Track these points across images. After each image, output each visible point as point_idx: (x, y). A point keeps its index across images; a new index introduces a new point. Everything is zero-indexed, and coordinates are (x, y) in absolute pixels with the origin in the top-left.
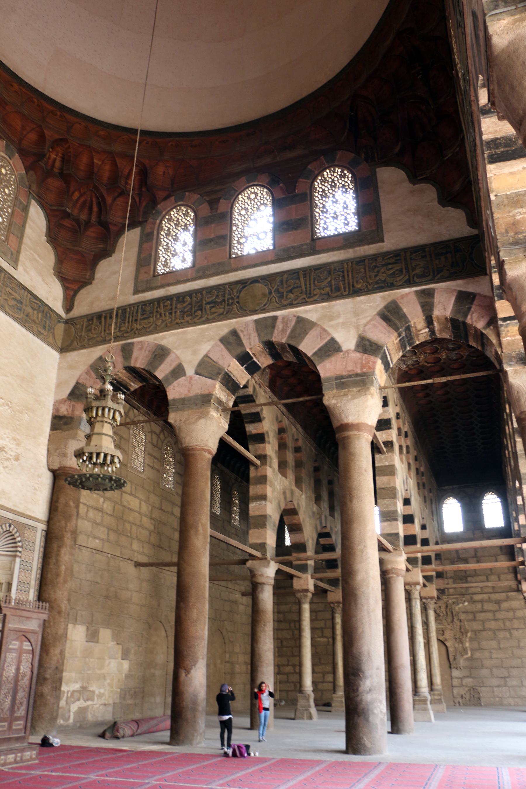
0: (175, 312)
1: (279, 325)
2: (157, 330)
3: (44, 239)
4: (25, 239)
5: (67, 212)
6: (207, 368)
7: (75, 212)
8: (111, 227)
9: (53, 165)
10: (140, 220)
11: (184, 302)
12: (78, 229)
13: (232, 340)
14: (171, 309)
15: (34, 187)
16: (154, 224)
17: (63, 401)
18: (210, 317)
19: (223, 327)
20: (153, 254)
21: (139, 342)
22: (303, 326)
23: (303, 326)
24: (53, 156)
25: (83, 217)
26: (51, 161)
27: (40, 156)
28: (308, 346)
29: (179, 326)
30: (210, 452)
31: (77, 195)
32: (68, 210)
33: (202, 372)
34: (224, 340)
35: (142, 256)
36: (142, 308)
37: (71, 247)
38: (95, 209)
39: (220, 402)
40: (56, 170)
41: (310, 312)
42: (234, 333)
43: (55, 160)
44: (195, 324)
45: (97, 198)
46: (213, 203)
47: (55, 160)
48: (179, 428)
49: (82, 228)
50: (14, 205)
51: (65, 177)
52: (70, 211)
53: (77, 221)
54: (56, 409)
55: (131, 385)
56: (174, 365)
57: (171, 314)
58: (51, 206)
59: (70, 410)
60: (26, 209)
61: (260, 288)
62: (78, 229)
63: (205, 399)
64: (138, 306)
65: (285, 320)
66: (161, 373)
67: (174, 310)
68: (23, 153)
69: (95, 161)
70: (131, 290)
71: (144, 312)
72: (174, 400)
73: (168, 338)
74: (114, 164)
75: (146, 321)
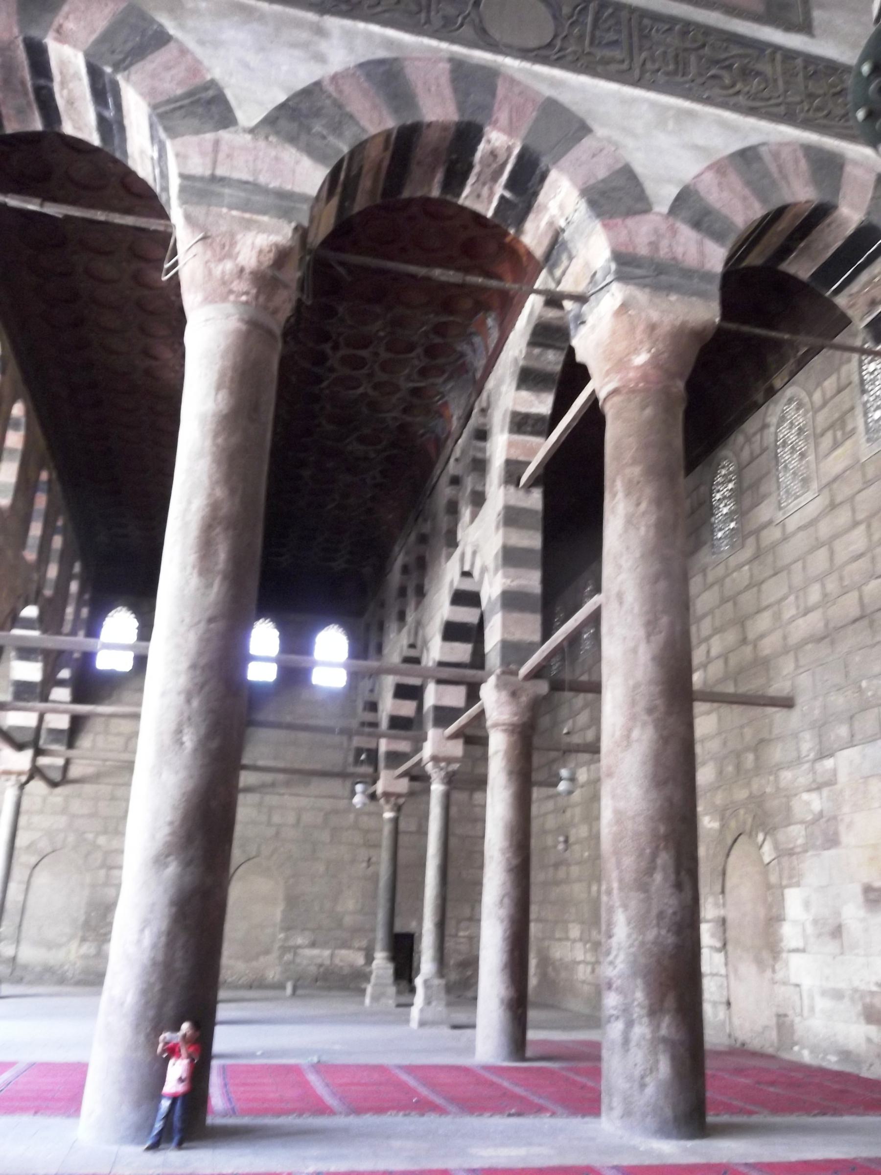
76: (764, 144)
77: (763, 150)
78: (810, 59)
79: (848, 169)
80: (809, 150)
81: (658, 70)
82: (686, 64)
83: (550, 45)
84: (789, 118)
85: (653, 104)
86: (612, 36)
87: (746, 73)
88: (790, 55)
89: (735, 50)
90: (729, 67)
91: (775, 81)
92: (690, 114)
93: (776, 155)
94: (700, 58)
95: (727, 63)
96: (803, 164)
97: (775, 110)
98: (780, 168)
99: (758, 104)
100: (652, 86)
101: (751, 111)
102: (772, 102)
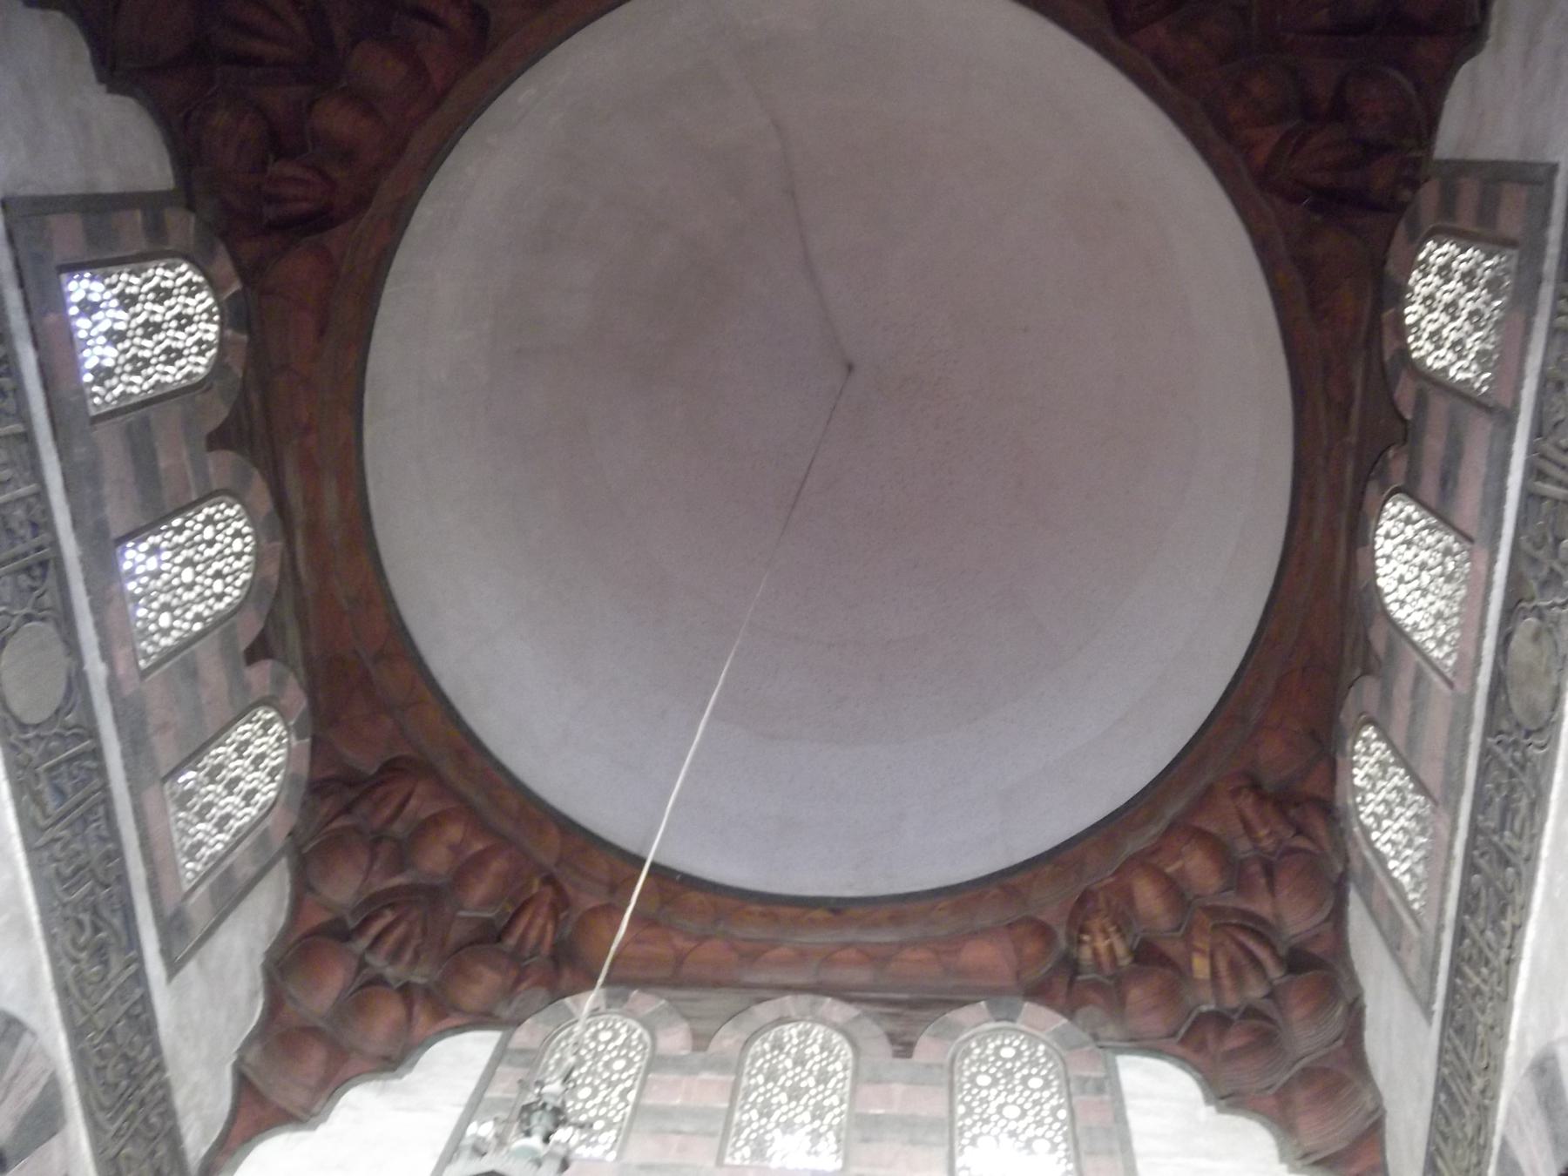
3: (1206, 1113)
4: (1138, 1145)
5: (1210, 1014)
7: (1231, 1000)
8: (1316, 950)
9: (1114, 959)
10: (1340, 869)
11: (1476, 896)
12: (1262, 1029)
15: (1110, 1030)
16: (1354, 840)
20: (1392, 894)
21: (1507, 1122)
24: (1102, 944)
25: (1255, 992)
26: (1105, 959)
27: (1070, 966)
31: (1200, 966)
32: (1204, 1008)
35: (1386, 926)
37: (1287, 1077)
38: (1262, 954)
40: (1125, 962)
43: (1111, 948)
45: (1243, 928)
47: (1111, 948)
49: (1276, 1016)
50: (1070, 1096)
51: (1148, 955)
52: (1212, 1007)
53: (1251, 1012)
58: (1173, 1035)
60: (1108, 1087)
62: (1262, 1029)
68: (1039, 992)
69: (1170, 870)
74: (1202, 835)
76: (34, 1034)
77: (26, 1039)
78: (146, 1000)
79: (55, 1142)
80: (54, 1083)
81: (58, 860)
82: (78, 885)
83: (24, 727)
84: (76, 1034)
85: (16, 883)
86: (68, 786)
87: (100, 952)
88: (140, 977)
89: (117, 921)
90: (97, 930)
91: (108, 986)
92: (26, 931)
93: (27, 1059)
94: (92, 892)
95: (101, 924)
96: (35, 1093)
97: (76, 1010)
98: (15, 1076)
99: (74, 990)
100: (35, 866)
101: (63, 991)
102: (85, 1002)
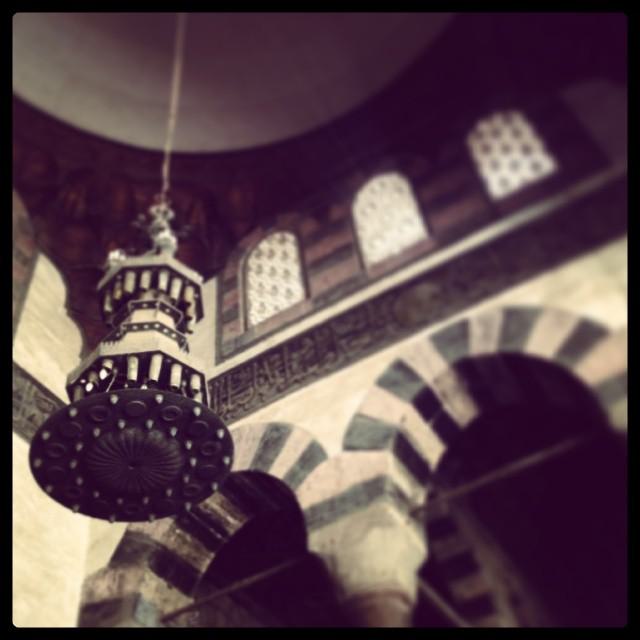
0: (290, 367)
1: (476, 331)
2: (263, 401)
6: (362, 435)
13: (400, 377)
14: (283, 365)
17: (103, 573)
18: (351, 354)
19: (380, 362)
22: (518, 321)
23: (518, 321)
28: (543, 343)
29: (301, 382)
30: (404, 598)
33: (356, 442)
34: (386, 383)
36: (232, 379)
39: (400, 496)
41: (526, 294)
42: (400, 366)
44: (328, 373)
46: (320, 213)
48: (333, 558)
54: (89, 592)
55: (228, 523)
56: (302, 447)
57: (283, 371)
59: (115, 588)
61: (425, 290)
63: (373, 489)
64: (226, 378)
65: (485, 322)
66: (279, 470)
67: (287, 365)
70: (212, 360)
71: (236, 382)
72: (314, 509)
73: (284, 409)
75: (242, 395)
